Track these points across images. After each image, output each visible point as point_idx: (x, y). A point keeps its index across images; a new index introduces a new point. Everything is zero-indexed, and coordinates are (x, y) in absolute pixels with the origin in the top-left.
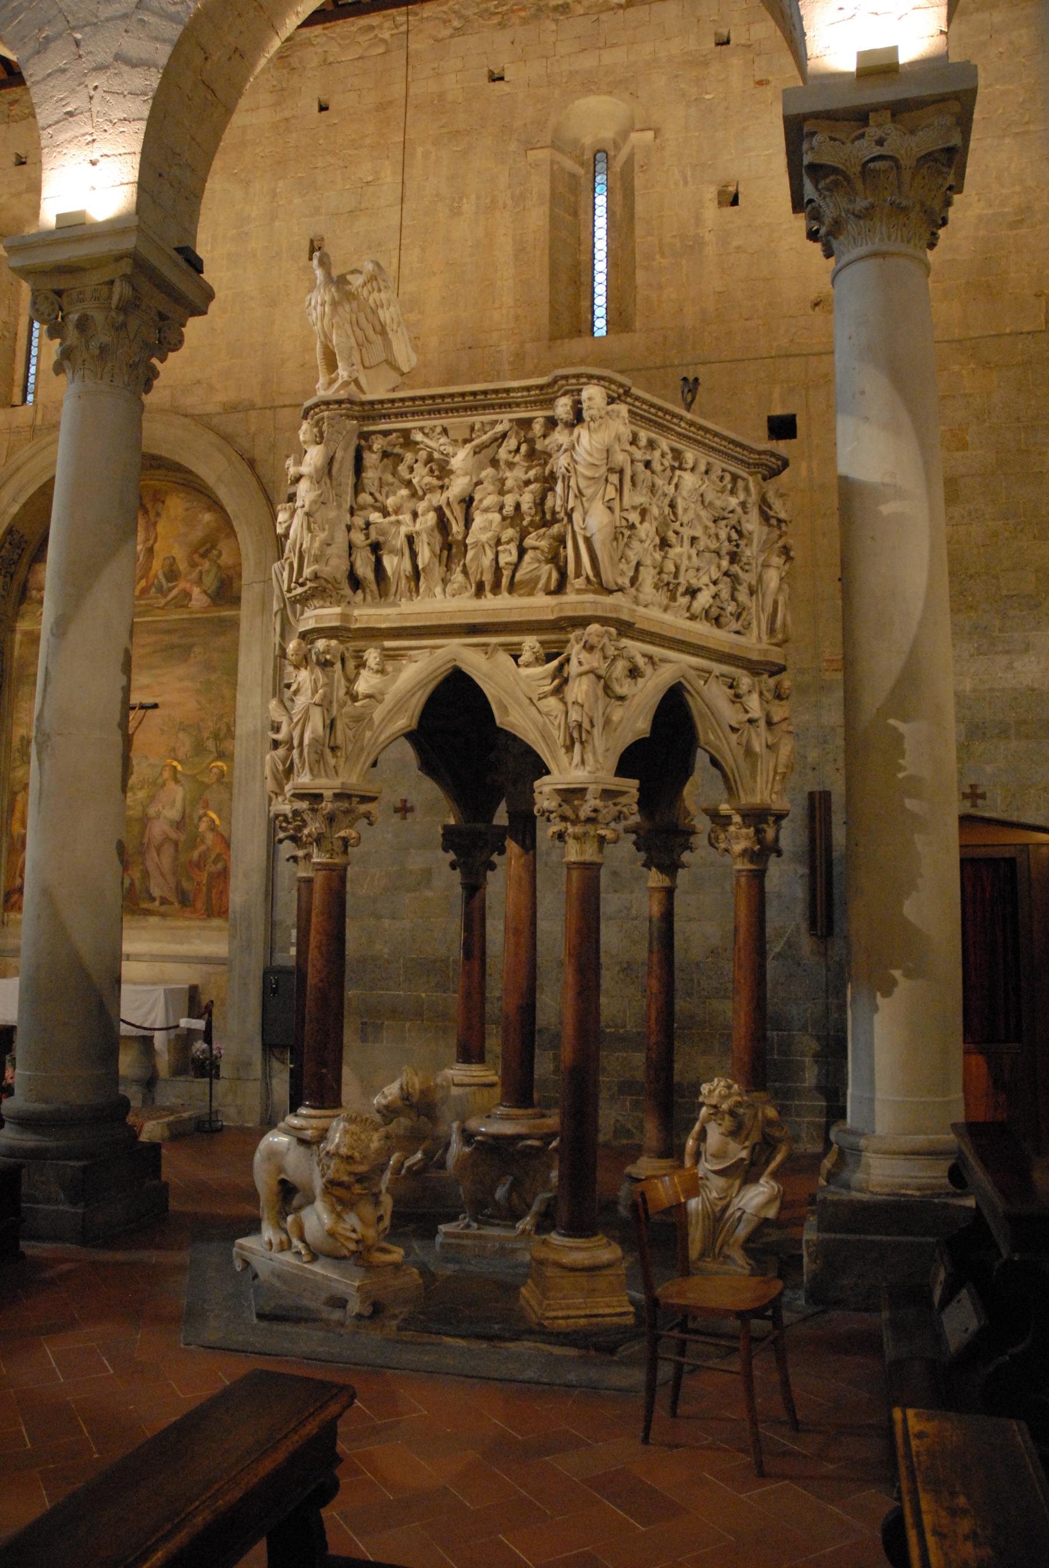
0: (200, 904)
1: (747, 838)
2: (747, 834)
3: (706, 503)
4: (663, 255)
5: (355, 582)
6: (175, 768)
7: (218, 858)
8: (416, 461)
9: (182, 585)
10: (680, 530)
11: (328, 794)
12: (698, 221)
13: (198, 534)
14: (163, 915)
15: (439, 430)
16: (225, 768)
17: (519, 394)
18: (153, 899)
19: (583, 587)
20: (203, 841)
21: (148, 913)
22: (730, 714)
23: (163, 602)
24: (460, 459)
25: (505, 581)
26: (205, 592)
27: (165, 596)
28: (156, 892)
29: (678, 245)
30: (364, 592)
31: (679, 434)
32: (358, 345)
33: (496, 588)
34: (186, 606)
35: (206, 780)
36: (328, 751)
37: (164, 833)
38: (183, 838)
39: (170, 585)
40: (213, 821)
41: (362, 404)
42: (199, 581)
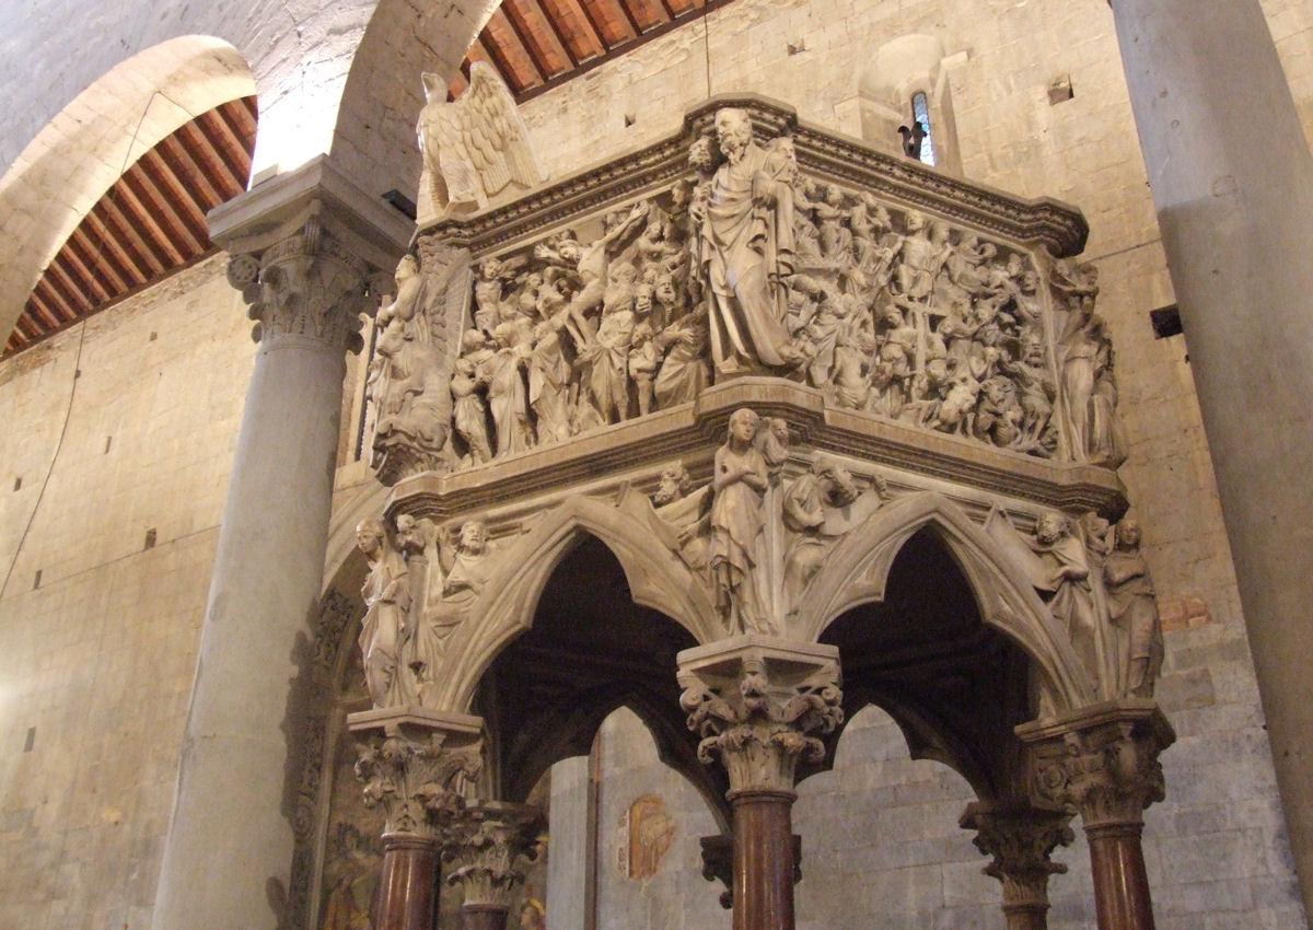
1: (1094, 770)
2: (1092, 762)
3: (956, 278)
4: (994, 167)
5: (462, 445)
8: (542, 282)
10: (910, 305)
11: (390, 726)
12: (1030, 124)
15: (566, 234)
17: (652, 159)
19: (733, 369)
22: (1037, 572)
24: (590, 259)
25: (644, 400)
29: (1011, 154)
30: (472, 456)
31: (896, 189)
32: (477, 169)
33: (634, 411)
36: (406, 670)
41: (471, 224)
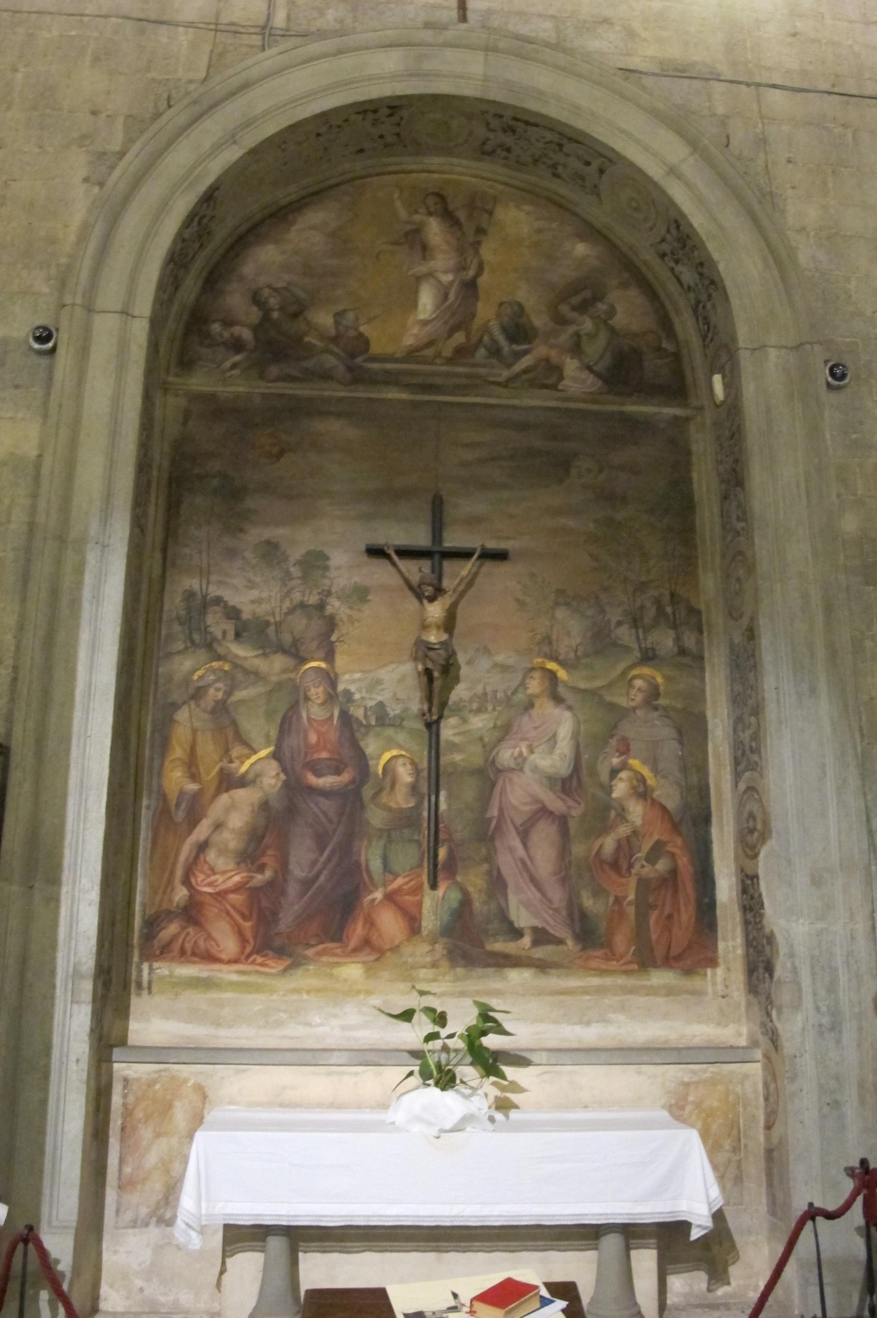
0: (621, 941)
6: (552, 675)
7: (657, 851)
9: (540, 350)
13: (564, 273)
14: (542, 966)
16: (660, 680)
18: (517, 933)
20: (622, 815)
21: (505, 961)
23: (505, 374)
26: (589, 368)
27: (509, 366)
28: (522, 918)
34: (554, 387)
35: (623, 701)
37: (536, 800)
38: (576, 812)
39: (516, 347)
40: (643, 780)
42: (576, 349)
